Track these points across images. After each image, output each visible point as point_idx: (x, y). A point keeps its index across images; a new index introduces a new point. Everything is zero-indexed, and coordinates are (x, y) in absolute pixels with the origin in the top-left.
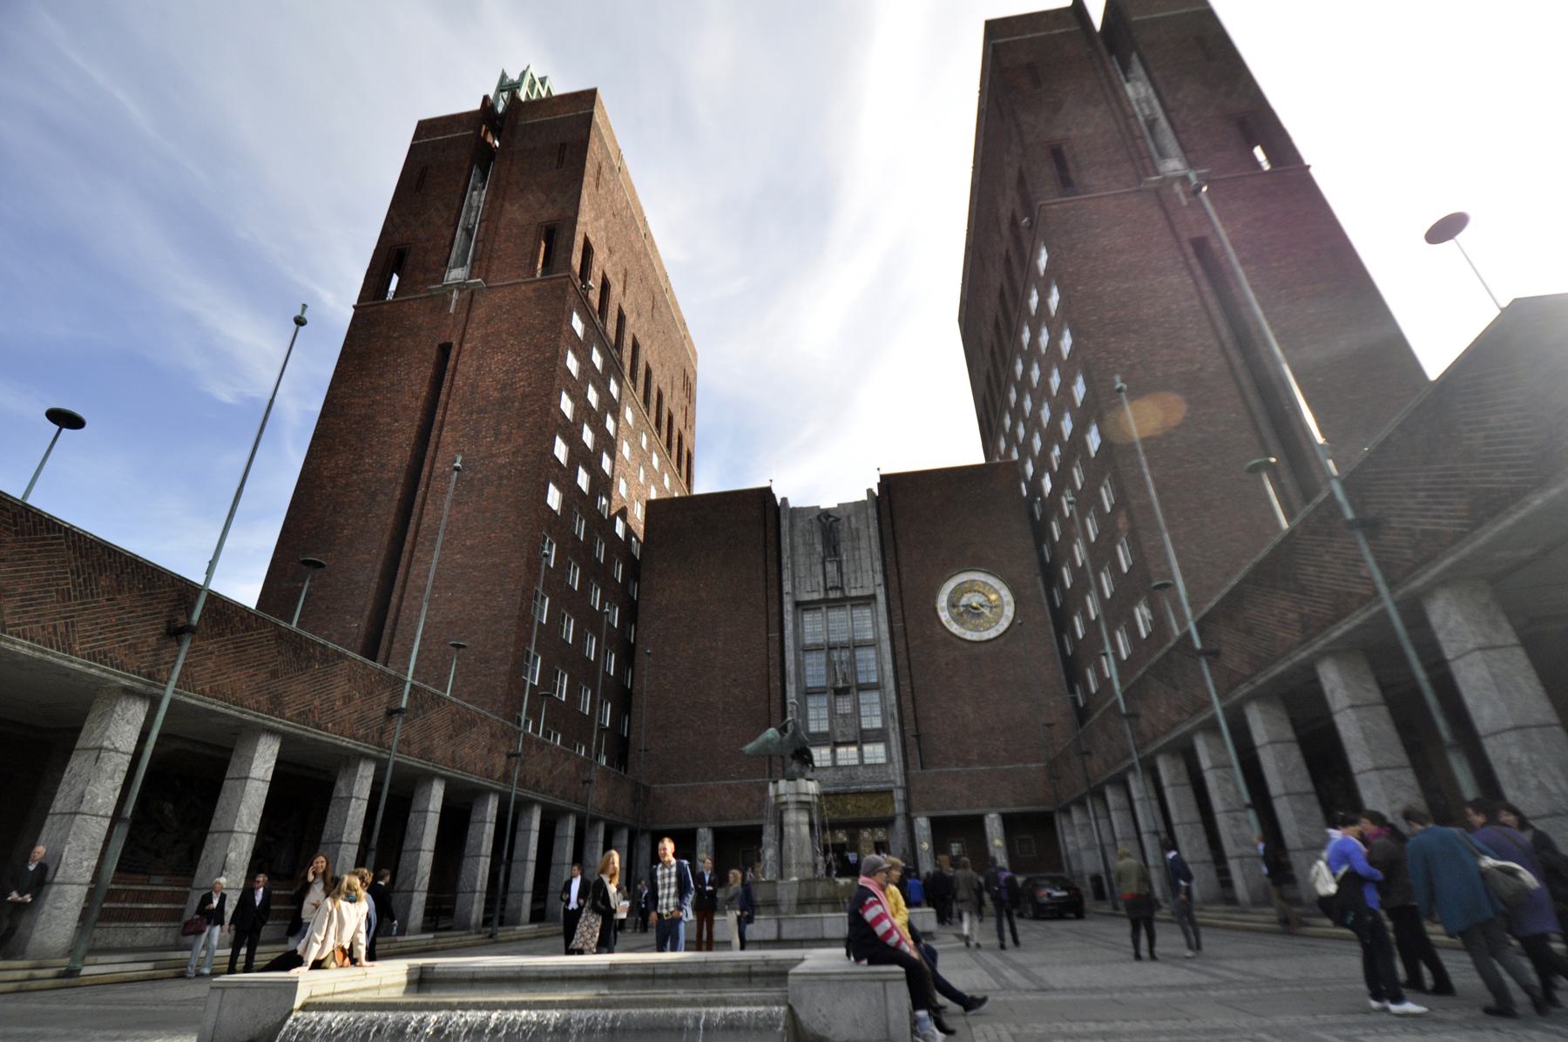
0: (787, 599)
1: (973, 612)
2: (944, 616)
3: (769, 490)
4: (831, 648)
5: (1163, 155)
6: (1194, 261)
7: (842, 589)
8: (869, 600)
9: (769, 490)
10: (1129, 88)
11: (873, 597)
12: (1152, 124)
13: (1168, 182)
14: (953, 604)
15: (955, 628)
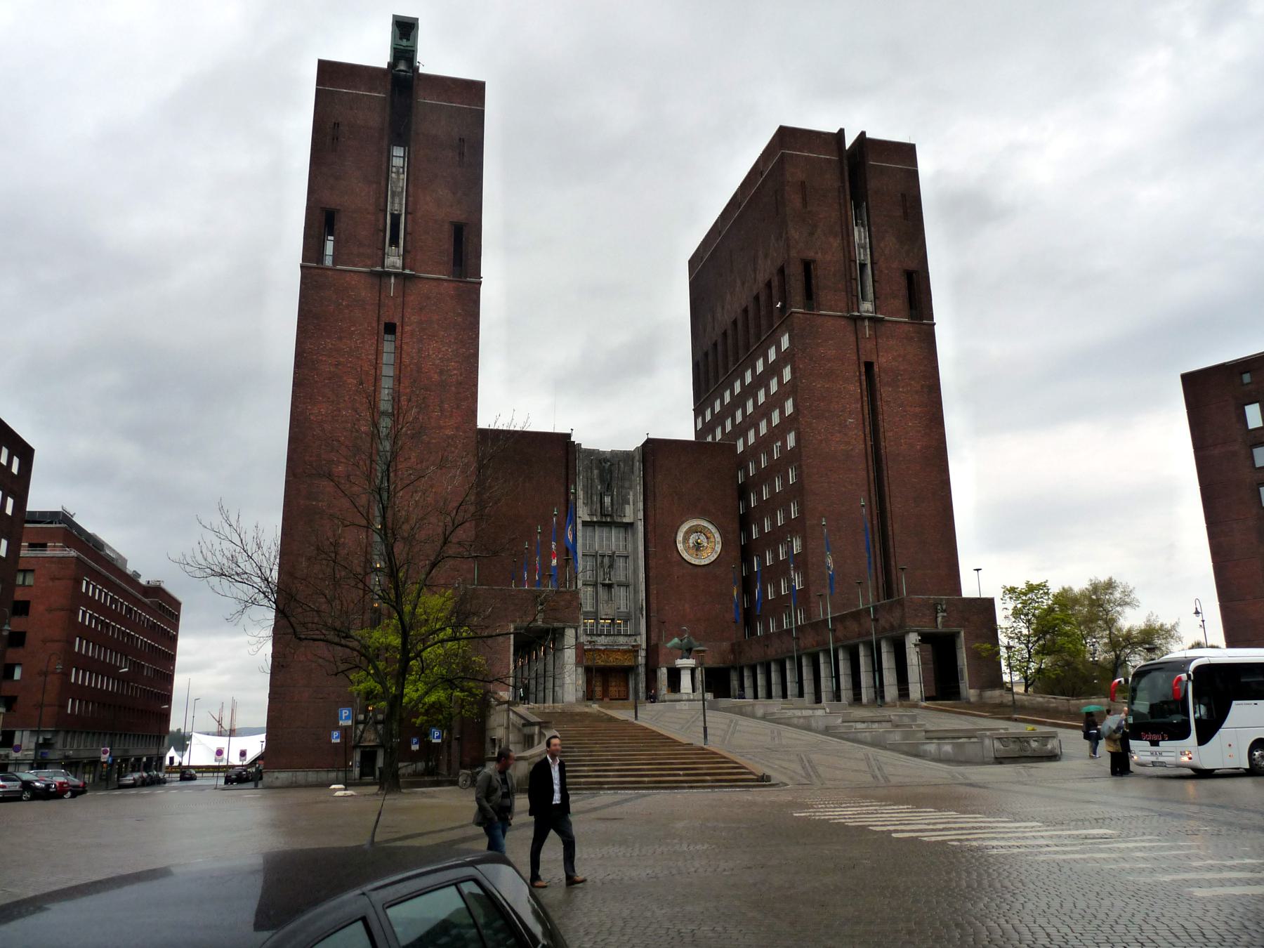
0: (579, 521)
1: (698, 546)
2: (680, 547)
3: (569, 436)
4: (603, 556)
5: (864, 299)
6: (863, 378)
7: (611, 516)
8: (630, 526)
9: (569, 436)
10: (856, 229)
11: (631, 524)
12: (863, 266)
13: (862, 318)
14: (686, 539)
15: (685, 556)
